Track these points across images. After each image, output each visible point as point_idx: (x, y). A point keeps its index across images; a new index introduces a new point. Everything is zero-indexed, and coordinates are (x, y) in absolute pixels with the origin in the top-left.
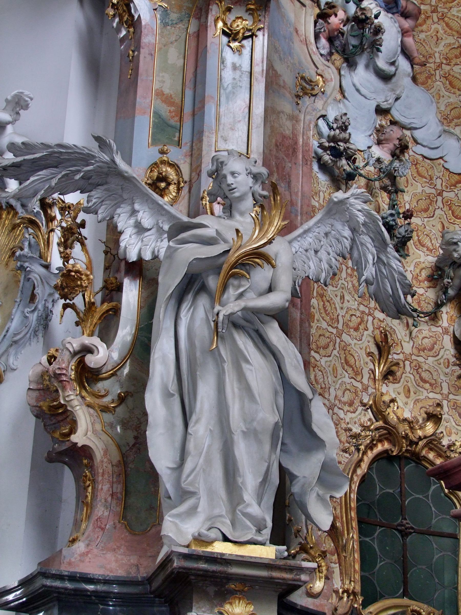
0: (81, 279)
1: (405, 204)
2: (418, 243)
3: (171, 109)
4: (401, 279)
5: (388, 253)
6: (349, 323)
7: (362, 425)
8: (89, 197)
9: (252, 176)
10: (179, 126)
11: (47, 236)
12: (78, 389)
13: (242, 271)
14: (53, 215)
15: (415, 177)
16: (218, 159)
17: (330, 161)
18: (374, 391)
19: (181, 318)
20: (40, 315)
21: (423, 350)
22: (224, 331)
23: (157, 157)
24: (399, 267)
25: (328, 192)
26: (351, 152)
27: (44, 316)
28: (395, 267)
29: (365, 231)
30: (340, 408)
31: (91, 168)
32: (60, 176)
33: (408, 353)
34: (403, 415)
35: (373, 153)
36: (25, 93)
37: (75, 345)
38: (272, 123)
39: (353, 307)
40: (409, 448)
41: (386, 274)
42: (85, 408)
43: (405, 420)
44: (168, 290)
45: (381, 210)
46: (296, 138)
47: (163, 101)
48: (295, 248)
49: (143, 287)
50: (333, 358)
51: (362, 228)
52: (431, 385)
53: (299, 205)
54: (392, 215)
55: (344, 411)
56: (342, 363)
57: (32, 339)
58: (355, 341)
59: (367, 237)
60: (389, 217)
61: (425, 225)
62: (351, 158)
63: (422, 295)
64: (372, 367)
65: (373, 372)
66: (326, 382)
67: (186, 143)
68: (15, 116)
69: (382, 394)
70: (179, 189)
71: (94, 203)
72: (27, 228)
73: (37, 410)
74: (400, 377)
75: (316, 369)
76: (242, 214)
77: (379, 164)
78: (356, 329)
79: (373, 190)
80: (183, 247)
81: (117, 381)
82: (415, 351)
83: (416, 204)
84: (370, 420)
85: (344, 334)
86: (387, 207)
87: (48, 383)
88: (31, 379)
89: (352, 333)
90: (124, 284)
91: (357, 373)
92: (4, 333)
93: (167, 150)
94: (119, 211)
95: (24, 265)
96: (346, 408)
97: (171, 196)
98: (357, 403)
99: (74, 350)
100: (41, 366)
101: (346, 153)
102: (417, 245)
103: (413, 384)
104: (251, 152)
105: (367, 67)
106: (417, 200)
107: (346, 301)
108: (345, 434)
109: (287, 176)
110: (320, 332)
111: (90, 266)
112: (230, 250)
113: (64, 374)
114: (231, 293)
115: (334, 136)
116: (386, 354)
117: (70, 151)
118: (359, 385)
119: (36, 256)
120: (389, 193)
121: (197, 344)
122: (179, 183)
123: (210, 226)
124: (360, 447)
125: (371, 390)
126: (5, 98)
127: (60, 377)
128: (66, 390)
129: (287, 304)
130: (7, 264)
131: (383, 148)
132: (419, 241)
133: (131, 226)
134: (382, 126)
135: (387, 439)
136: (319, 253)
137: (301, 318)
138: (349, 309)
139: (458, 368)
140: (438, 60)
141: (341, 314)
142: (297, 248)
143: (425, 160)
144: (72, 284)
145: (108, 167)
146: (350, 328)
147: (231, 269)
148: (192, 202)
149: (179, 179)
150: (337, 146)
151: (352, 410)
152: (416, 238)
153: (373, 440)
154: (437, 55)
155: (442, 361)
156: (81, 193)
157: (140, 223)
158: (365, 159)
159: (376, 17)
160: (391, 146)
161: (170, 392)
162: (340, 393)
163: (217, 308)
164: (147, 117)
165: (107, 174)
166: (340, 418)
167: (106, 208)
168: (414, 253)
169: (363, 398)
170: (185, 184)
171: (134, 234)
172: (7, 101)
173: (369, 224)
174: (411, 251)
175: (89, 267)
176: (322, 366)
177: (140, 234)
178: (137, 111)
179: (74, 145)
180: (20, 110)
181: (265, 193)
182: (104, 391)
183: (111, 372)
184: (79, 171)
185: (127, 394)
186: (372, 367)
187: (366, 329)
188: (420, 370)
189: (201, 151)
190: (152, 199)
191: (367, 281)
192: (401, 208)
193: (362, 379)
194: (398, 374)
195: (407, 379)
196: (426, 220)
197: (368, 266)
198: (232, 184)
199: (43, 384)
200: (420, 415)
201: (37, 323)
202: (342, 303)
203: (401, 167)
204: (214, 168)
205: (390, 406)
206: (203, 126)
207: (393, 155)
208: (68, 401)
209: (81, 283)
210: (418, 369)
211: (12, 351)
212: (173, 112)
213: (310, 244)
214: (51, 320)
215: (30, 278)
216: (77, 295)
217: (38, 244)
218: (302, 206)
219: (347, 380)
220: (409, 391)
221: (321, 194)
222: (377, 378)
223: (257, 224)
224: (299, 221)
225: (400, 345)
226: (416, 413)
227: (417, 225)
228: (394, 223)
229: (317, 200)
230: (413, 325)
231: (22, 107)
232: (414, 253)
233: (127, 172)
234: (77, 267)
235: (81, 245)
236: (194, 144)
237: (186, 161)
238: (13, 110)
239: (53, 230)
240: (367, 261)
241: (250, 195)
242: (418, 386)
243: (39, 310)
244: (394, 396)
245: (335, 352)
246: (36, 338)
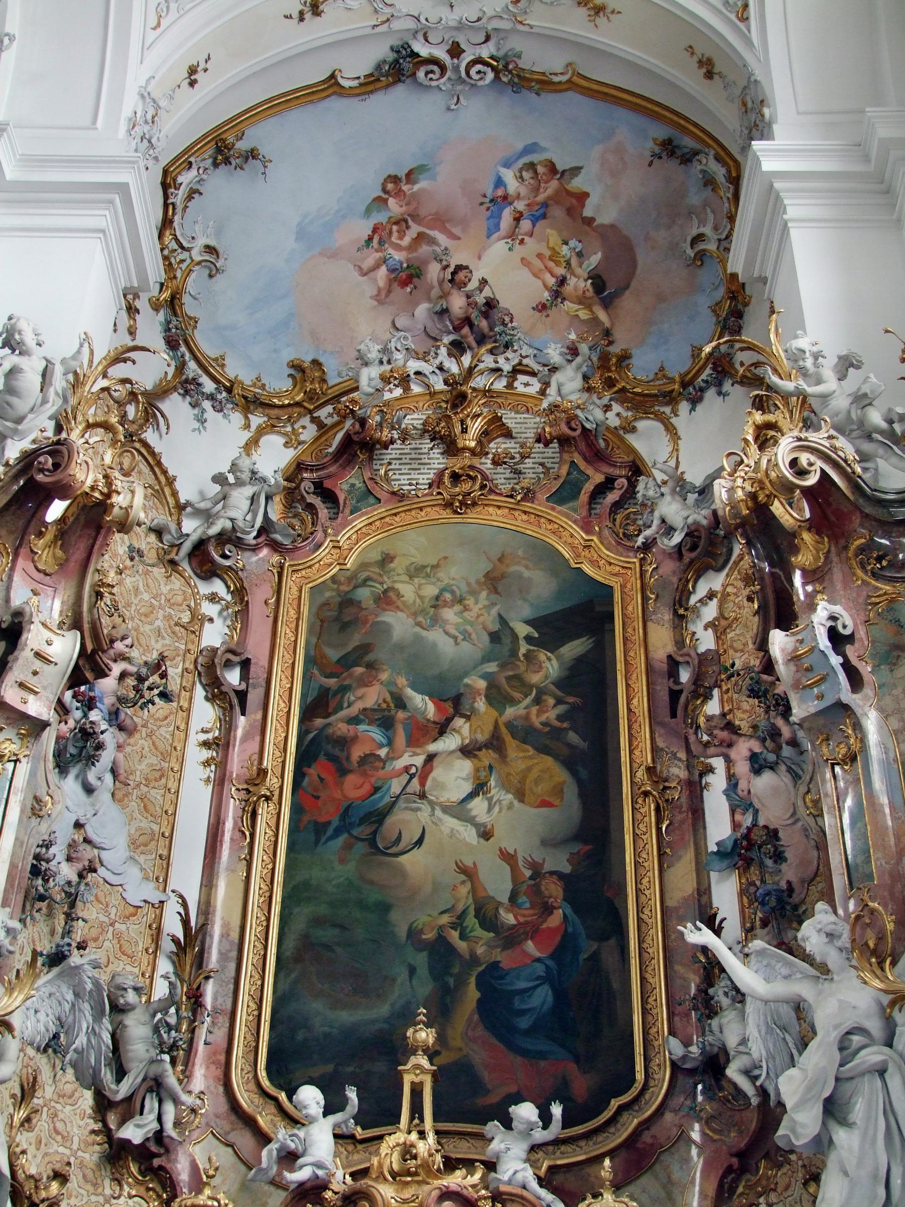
21: (64, 1096)
43: (32, 1177)
52: (63, 1137)
65: (12, 1117)
82: (55, 1097)
105: (77, 777)
134: (74, 841)
139: (92, 1121)
140: (138, 779)
154: (138, 773)
155: (78, 1111)
159: (102, 733)
160: (80, 866)
194: (34, 1121)
207: (81, 876)
226: (42, 1169)
240: (80, 1028)
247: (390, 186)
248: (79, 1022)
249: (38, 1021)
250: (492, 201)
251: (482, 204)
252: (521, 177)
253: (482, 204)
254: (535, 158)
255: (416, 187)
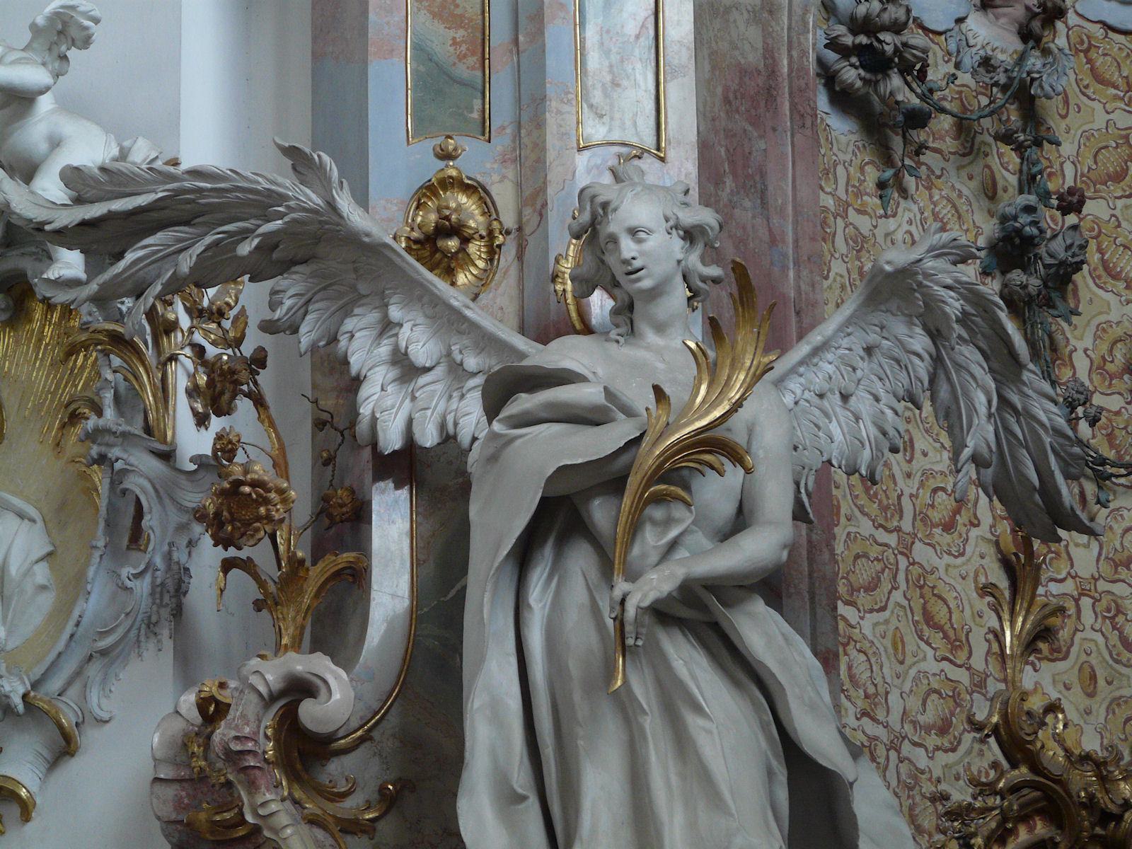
0: (266, 501)
1: (1062, 164)
2: (1101, 271)
3: (457, 36)
4: (1061, 445)
5: (1025, 384)
6: (930, 512)
7: (974, 782)
8: (274, 292)
9: (681, 233)
10: (479, 81)
11: (160, 375)
12: (284, 783)
13: (672, 488)
14: (171, 316)
15: (1087, 87)
16: (593, 198)
17: (859, 84)
18: (1002, 686)
19: (529, 606)
20: (159, 581)
22: (640, 643)
23: (432, 168)
24: (1053, 416)
25: (857, 162)
26: (914, 56)
27: (171, 585)
28: (1044, 418)
29: (965, 335)
30: (915, 744)
31: (277, 224)
32: (199, 248)
33: (1088, 576)
34: (1079, 743)
35: (970, 35)
36: (82, 9)
37: (269, 677)
38: (714, 44)
39: (937, 468)
40: (1098, 830)
41: (1021, 438)
42: (305, 828)
43: (1086, 758)
44: (498, 547)
45: (1000, 192)
46: (773, 58)
47: (434, 15)
48: (793, 392)
49: (420, 510)
50: (892, 612)
51: (958, 329)
53: (790, 238)
54: (1029, 209)
55: (926, 750)
56: (916, 623)
57: (142, 644)
58: (947, 559)
59: (971, 348)
60: (1021, 215)
61: (1117, 219)
62: (914, 69)
63: (1118, 413)
64: (994, 623)
65: (998, 636)
66: (878, 680)
67: (503, 128)
68: (57, 64)
69: (1024, 697)
70: (493, 252)
71: (290, 309)
72: (106, 354)
73: (179, 832)
74: (1069, 641)
75: (850, 648)
76: (660, 328)
77: (988, 72)
78: (949, 527)
79: (974, 137)
80: (526, 435)
81: (375, 754)
82: (1106, 569)
83: (1090, 162)
84: (995, 765)
85: (918, 545)
86: (1013, 180)
87: (203, 763)
88: (159, 755)
89: (937, 538)
90: (374, 506)
91: (957, 643)
92: (69, 628)
93: (455, 149)
94: (349, 324)
95: (110, 455)
96: (933, 740)
97: (475, 272)
98: (959, 723)
99: (270, 691)
100: (180, 719)
101: (901, 58)
102: (1099, 277)
103: (1104, 658)
104: (668, 142)
106: (1094, 151)
107: (918, 454)
108: (931, 810)
109: (757, 178)
110: (857, 549)
111: (281, 465)
112: (642, 435)
113: (249, 752)
114: (651, 540)
115: (867, 18)
116: (1028, 587)
117: (222, 185)
118: (962, 676)
119: (137, 429)
120: (1020, 148)
121: (574, 668)
122: (491, 233)
123: (590, 376)
124: (973, 841)
125: (993, 686)
126: (30, 21)
127: (240, 759)
128: (257, 788)
129: (785, 555)
130: (58, 445)
131: (997, 18)
132: (1105, 263)
133: (384, 363)
135: (1041, 812)
136: (853, 400)
137: (810, 541)
138: (927, 474)
141: (907, 492)
142: (799, 392)
143: (1111, 34)
144: (246, 514)
145: (320, 222)
146: (933, 526)
147: (647, 486)
148: (529, 284)
149: (490, 225)
150: (875, 44)
151: (947, 745)
152: (1097, 256)
153: (1005, 819)
156: (251, 280)
157: (406, 354)
158: (949, 54)
160: (1018, 12)
161: (515, 791)
162: (914, 703)
163: (621, 586)
164: (397, 61)
165: (317, 240)
166: (917, 769)
167: (319, 319)
168: (1091, 300)
169: (974, 710)
170: (508, 237)
171: (394, 381)
172: (34, 27)
173: (974, 318)
174: (1084, 294)
175: (281, 461)
176: (865, 637)
177: (405, 382)
178: (371, 49)
179: (231, 170)
180: (68, 49)
181: (714, 271)
182: (344, 782)
183: (359, 733)
184: (244, 234)
185: (405, 785)
186: (994, 623)
187: (975, 523)
188: (1120, 619)
189: (544, 149)
190: (433, 294)
191: (976, 459)
192: (1054, 179)
193: (969, 658)
194: (1064, 635)
195: (1087, 645)
196: (1120, 203)
197: (976, 421)
198: (633, 258)
199: (189, 766)
200: (1126, 739)
201: (154, 603)
202: (910, 461)
203: (1048, 69)
204: (586, 217)
205: (1045, 724)
206: (544, 84)
207: (1026, 35)
208: (264, 817)
209: (268, 510)
210: (1116, 615)
211: (93, 670)
212: (463, 42)
213: (830, 378)
214: (186, 592)
215: (127, 489)
216: (260, 540)
217: (137, 396)
218: (796, 241)
219: (931, 666)
220: (1093, 677)
221: (840, 169)
222: (1008, 652)
223: (704, 366)
224: (792, 281)
225: (1064, 555)
227: (1096, 220)
228: (1035, 231)
229: (828, 190)
230: (1098, 502)
231: (73, 40)
232: (1091, 300)
233: (368, 235)
234: (256, 472)
235: (255, 405)
236: (523, 132)
237: (504, 177)
238: (50, 49)
239: (173, 358)
240: (972, 409)
241: (679, 278)
242: (1117, 662)
243: (157, 570)
244: (1054, 695)
245: (897, 596)
246: (153, 640)
248: (966, 394)
249: (857, 418)
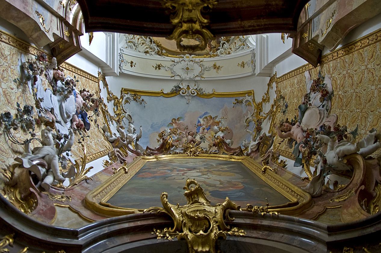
247: (174, 121)
250: (197, 126)
251: (195, 126)
252: (204, 120)
253: (195, 126)
254: (207, 115)
255: (180, 122)
